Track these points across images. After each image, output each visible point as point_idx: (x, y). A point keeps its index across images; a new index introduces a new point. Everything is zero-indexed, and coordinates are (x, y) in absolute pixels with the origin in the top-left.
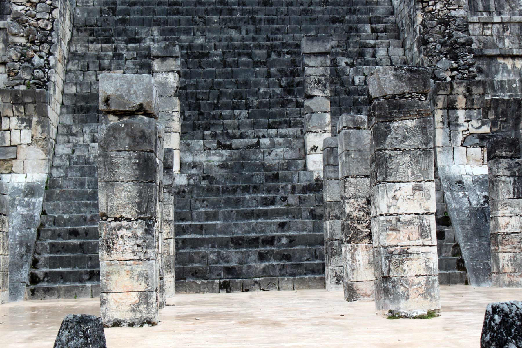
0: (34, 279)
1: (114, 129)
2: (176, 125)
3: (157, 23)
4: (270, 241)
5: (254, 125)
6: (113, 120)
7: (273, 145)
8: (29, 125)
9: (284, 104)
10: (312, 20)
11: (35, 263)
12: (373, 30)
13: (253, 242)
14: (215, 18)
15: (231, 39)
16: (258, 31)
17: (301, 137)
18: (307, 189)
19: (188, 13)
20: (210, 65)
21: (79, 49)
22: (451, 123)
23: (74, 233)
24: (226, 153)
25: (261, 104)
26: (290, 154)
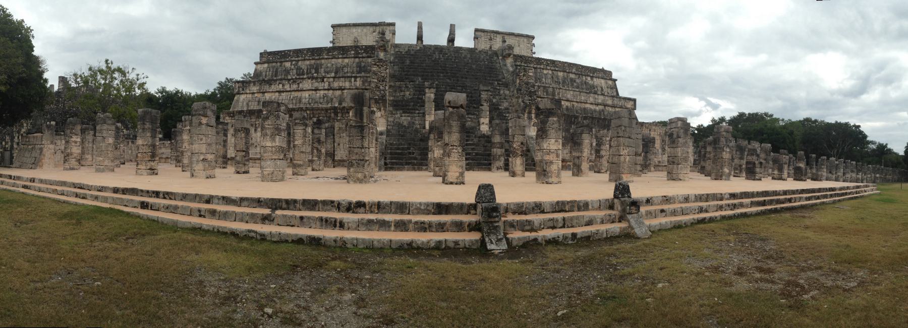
0: (386, 164)
1: (452, 113)
6: (451, 109)
11: (385, 159)
21: (392, 84)
23: (398, 149)
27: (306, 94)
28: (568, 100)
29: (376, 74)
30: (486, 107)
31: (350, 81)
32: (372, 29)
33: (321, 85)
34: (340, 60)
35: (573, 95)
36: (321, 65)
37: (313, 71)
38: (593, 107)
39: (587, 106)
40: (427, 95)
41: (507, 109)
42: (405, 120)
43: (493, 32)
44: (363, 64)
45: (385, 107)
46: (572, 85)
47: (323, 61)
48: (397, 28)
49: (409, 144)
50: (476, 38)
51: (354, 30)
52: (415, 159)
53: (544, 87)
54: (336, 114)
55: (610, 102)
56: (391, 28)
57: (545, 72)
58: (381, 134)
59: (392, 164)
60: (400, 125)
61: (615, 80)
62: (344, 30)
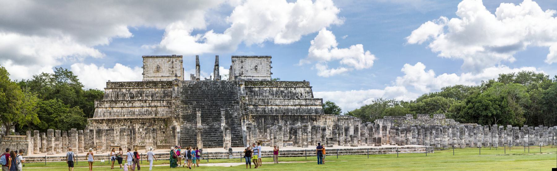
22: (244, 122)
27: (137, 110)
28: (276, 105)
30: (223, 118)
32: (168, 59)
33: (144, 105)
34: (154, 89)
36: (144, 92)
38: (292, 108)
39: (290, 107)
41: (236, 117)
42: (188, 125)
43: (243, 57)
46: (282, 94)
51: (157, 60)
54: (155, 121)
55: (304, 103)
56: (180, 58)
57: (265, 89)
58: (178, 133)
60: (186, 128)
61: (311, 87)
62: (150, 60)
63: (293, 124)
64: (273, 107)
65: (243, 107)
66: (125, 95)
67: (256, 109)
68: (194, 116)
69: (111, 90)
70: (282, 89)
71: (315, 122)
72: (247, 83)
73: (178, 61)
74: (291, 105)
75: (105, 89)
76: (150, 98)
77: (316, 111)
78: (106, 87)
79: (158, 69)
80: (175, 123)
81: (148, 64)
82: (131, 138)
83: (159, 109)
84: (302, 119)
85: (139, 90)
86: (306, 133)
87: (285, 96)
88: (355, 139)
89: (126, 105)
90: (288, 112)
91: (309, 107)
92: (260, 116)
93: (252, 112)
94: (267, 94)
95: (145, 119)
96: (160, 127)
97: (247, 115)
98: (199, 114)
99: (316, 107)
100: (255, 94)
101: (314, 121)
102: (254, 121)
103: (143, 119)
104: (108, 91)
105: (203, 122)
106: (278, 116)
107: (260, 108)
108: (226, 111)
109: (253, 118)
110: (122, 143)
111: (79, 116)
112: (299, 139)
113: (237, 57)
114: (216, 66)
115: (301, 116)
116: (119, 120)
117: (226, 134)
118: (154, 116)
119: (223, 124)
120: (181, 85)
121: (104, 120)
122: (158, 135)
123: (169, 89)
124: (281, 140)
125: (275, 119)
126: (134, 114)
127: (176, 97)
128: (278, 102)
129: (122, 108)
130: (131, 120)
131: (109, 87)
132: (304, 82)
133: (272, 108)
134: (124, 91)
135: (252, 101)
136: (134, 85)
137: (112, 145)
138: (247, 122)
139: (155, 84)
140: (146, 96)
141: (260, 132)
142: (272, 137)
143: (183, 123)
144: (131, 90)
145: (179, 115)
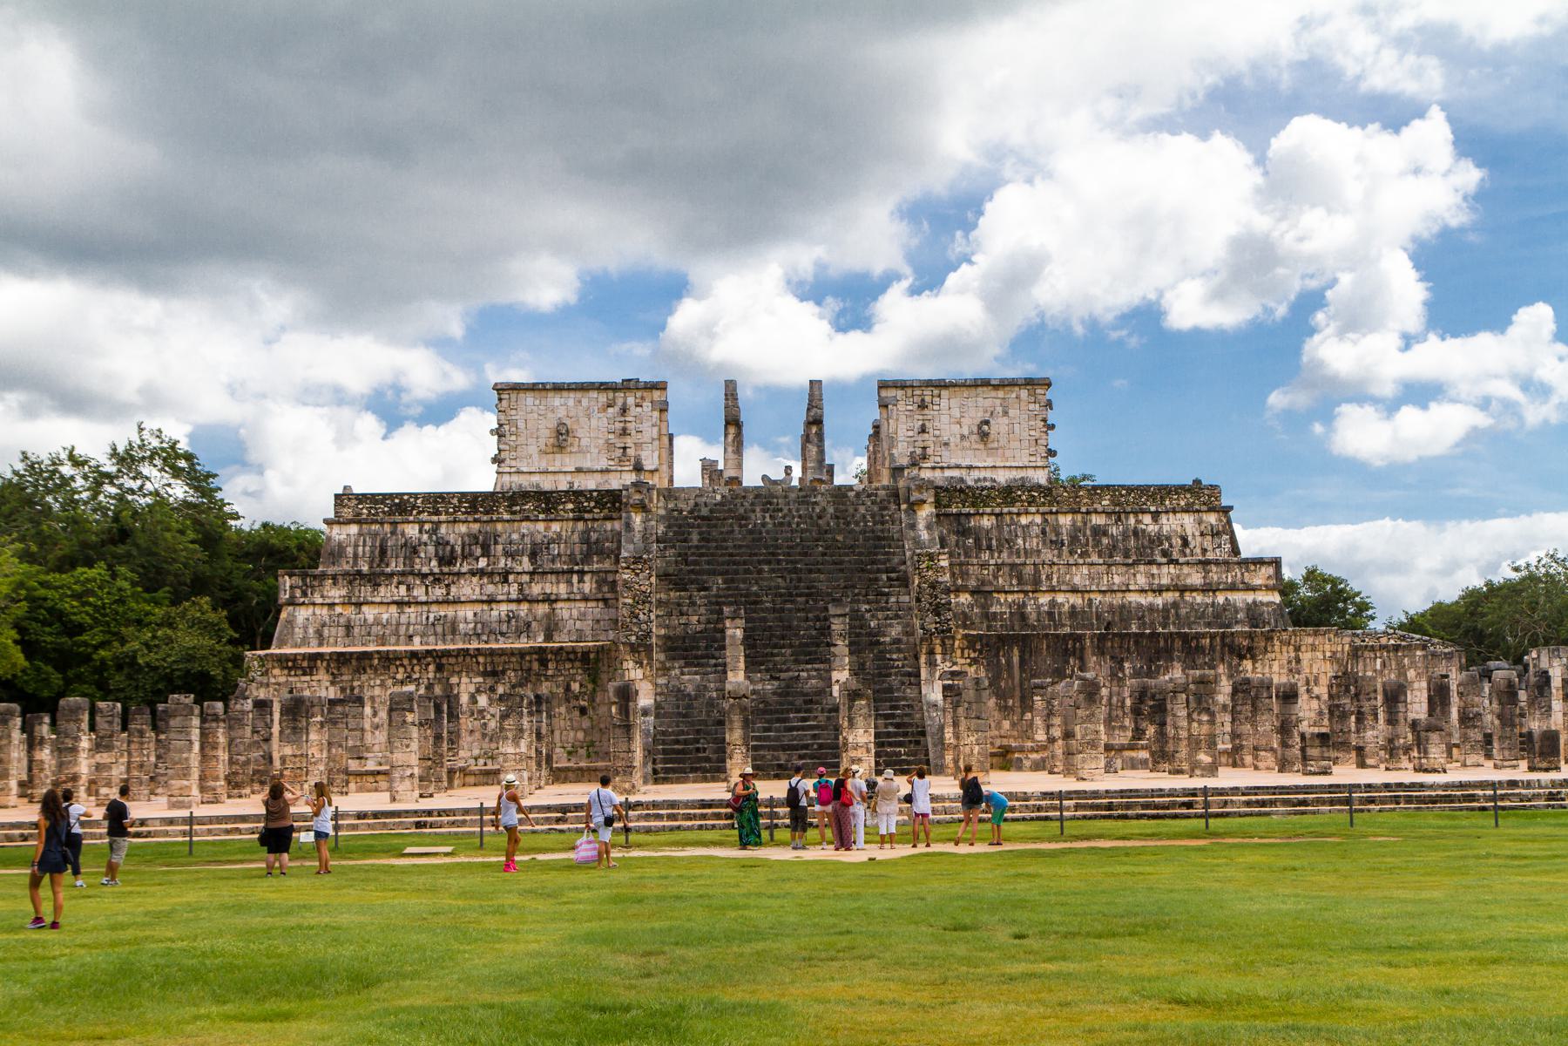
0: (655, 771)
2: (742, 665)
3: (721, 574)
4: (806, 747)
5: (797, 662)
7: (809, 677)
8: (641, 665)
9: (818, 645)
10: (842, 570)
11: (654, 762)
12: (889, 579)
13: (795, 748)
14: (766, 568)
15: (778, 587)
16: (800, 580)
17: (829, 671)
18: (830, 711)
19: (745, 563)
20: (762, 610)
22: (932, 664)
23: (677, 742)
24: (776, 683)
25: (801, 645)
26: (821, 684)
27: (467, 612)
28: (1074, 591)
29: (629, 589)
30: (841, 647)
31: (569, 582)
32: (603, 398)
33: (500, 591)
34: (541, 526)
35: (1091, 578)
36: (496, 536)
37: (478, 551)
38: (1144, 600)
39: (1133, 598)
40: (729, 632)
41: (897, 641)
42: (690, 680)
43: (929, 384)
44: (594, 536)
45: (650, 658)
46: (1098, 543)
47: (499, 526)
48: (672, 394)
49: (698, 732)
50: (884, 405)
51: (556, 400)
52: (708, 760)
53: (1013, 566)
54: (544, 663)
55: (1196, 578)
56: (656, 394)
57: (1024, 520)
58: (645, 712)
59: (667, 771)
60: (679, 693)
61: (1226, 510)
62: (529, 399)
63: (1149, 674)
64: (1060, 598)
65: (925, 598)
66: (415, 551)
67: (984, 607)
68: (714, 640)
69: (354, 529)
70: (1098, 520)
71: (1247, 664)
72: (946, 494)
73: (647, 405)
74: (1139, 589)
75: (327, 522)
76: (526, 564)
77: (1254, 614)
78: (331, 515)
79: (562, 438)
80: (633, 672)
81: (519, 416)
82: (438, 738)
83: (563, 611)
84: (1191, 649)
85: (476, 526)
86: (1207, 710)
87: (1113, 548)
88: (1434, 737)
89: (419, 593)
90: (1125, 622)
91: (1220, 599)
92: (1000, 638)
93: (965, 619)
94: (1034, 543)
95: (502, 652)
96: (568, 689)
97: (945, 634)
98: (735, 632)
99: (1250, 597)
100: (982, 541)
101: (1242, 657)
102: (974, 661)
103: (492, 652)
104: (339, 534)
105: (752, 664)
106: (1079, 638)
107: (1002, 605)
108: (856, 616)
109: (971, 646)
110: (398, 757)
111: (208, 642)
112: (1177, 739)
113: (901, 385)
114: (809, 424)
115: (1185, 638)
116: (388, 660)
117: (851, 720)
118: (540, 641)
119: (841, 675)
120: (659, 507)
121: (319, 656)
122: (559, 723)
123: (608, 525)
124: (1093, 744)
125: (1067, 649)
126: (454, 631)
127: (638, 560)
128: (1079, 577)
129: (400, 604)
130: (439, 660)
131: (347, 513)
132: (1196, 488)
133: (1053, 603)
134: (412, 531)
135: (965, 575)
136: (457, 509)
137: (354, 765)
138: (947, 666)
139: (547, 502)
140: (507, 554)
141: (1004, 709)
142: (1057, 732)
143: (665, 670)
144: (443, 529)
145: (648, 634)
